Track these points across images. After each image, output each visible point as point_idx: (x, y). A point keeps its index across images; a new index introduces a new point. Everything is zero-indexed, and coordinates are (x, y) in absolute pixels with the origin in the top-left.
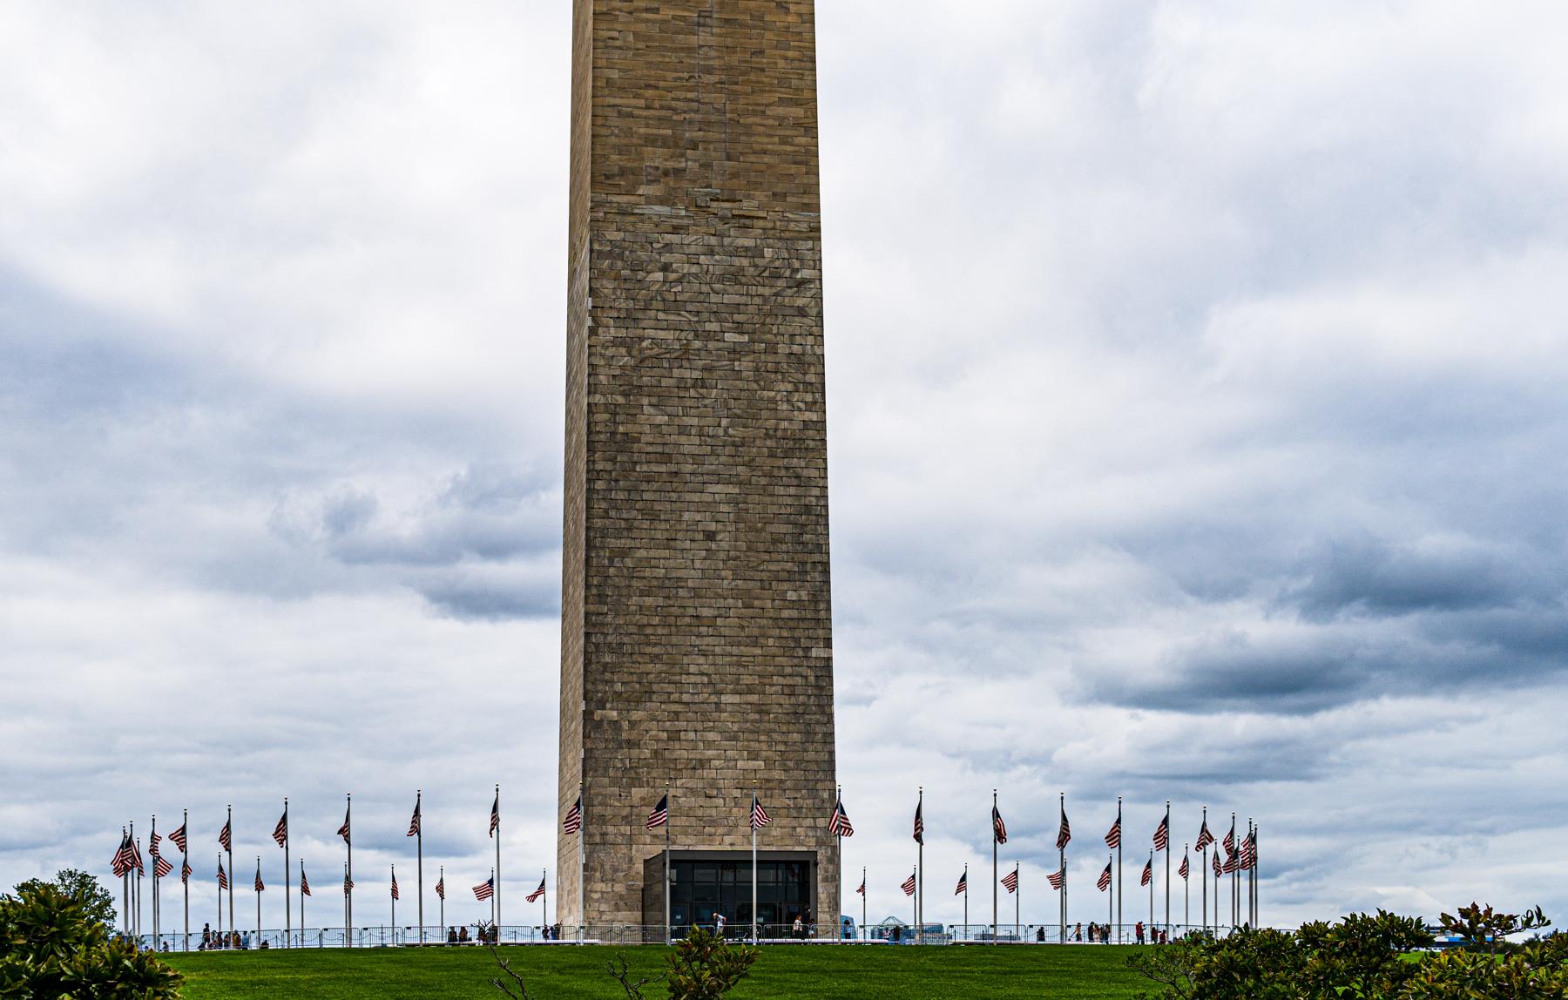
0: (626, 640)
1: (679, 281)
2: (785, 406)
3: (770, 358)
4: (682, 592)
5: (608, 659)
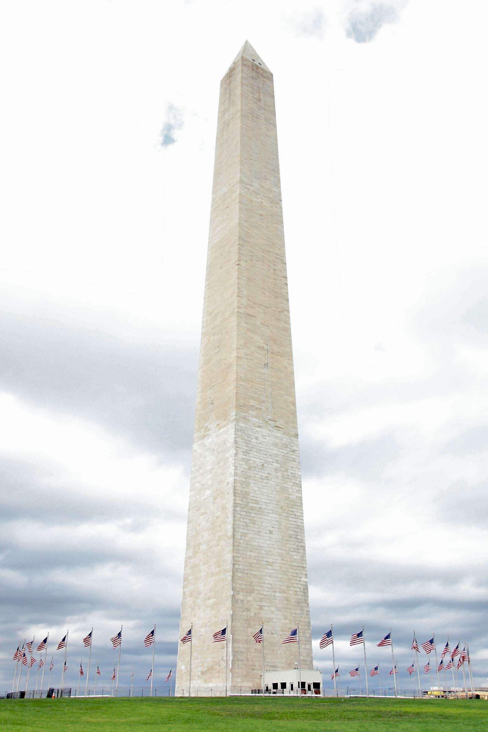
0: (246, 568)
1: (260, 443)
5: (240, 575)
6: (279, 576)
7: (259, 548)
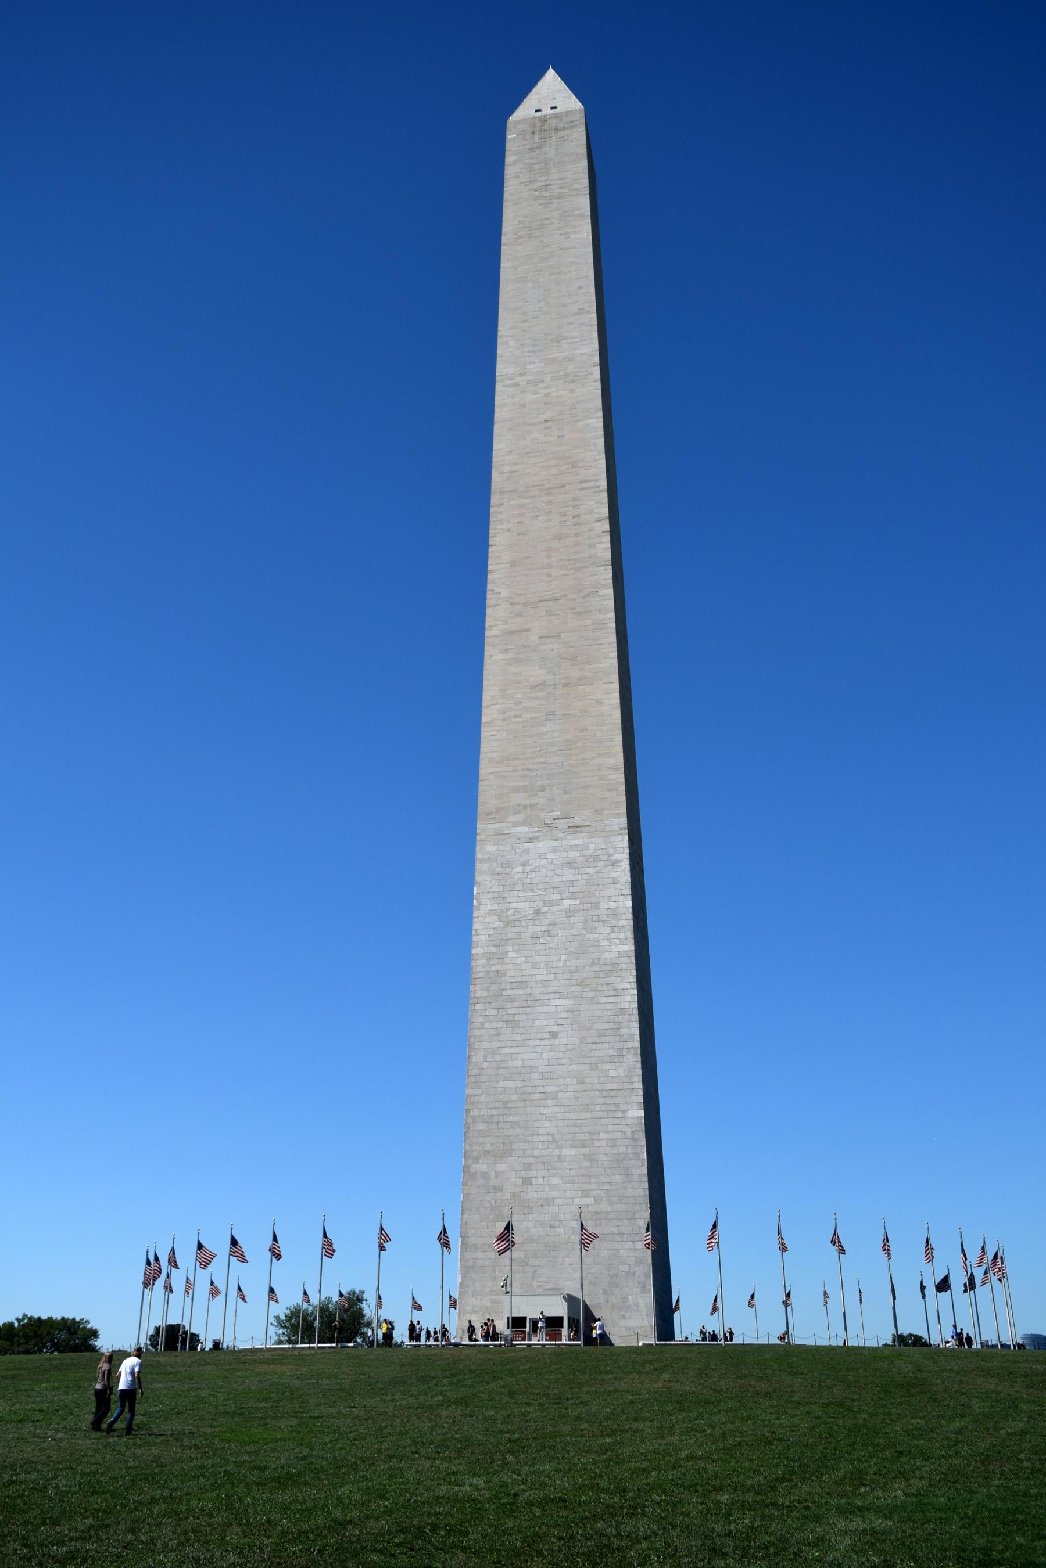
0: (494, 1112)
2: (605, 943)
3: (595, 912)
4: (535, 1076)
6: (572, 1115)
7: (524, 1070)
